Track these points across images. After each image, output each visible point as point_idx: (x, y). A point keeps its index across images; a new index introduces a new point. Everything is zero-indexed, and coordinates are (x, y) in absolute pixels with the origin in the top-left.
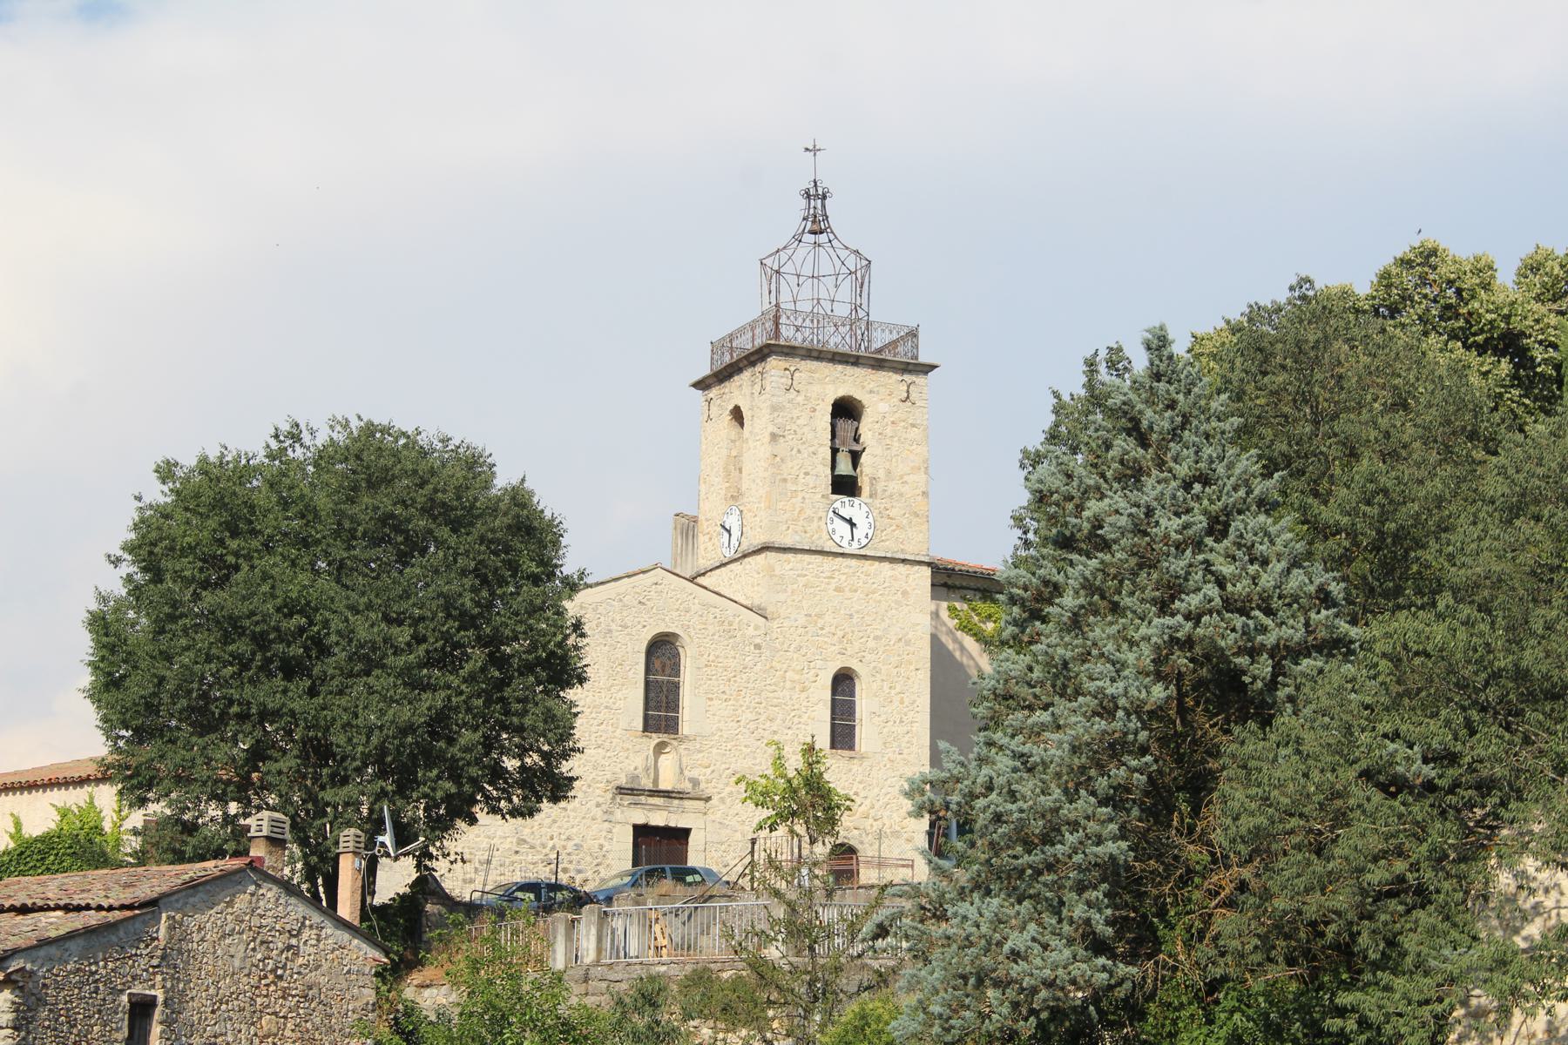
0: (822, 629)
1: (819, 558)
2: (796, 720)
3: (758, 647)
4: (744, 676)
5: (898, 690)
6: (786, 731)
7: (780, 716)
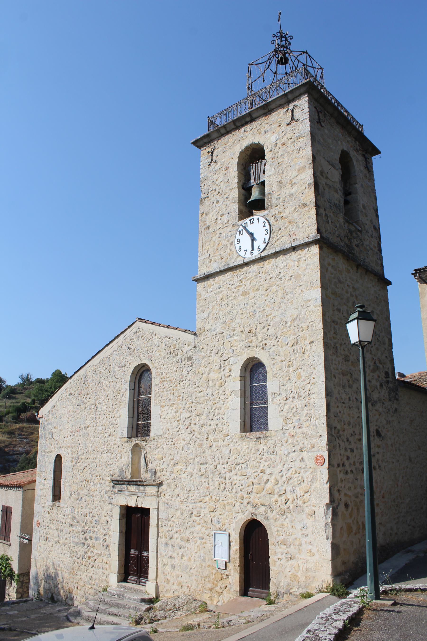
0: (234, 330)
1: (230, 274)
2: (217, 412)
3: (190, 359)
4: (182, 384)
5: (295, 367)
6: (209, 422)
7: (206, 411)
